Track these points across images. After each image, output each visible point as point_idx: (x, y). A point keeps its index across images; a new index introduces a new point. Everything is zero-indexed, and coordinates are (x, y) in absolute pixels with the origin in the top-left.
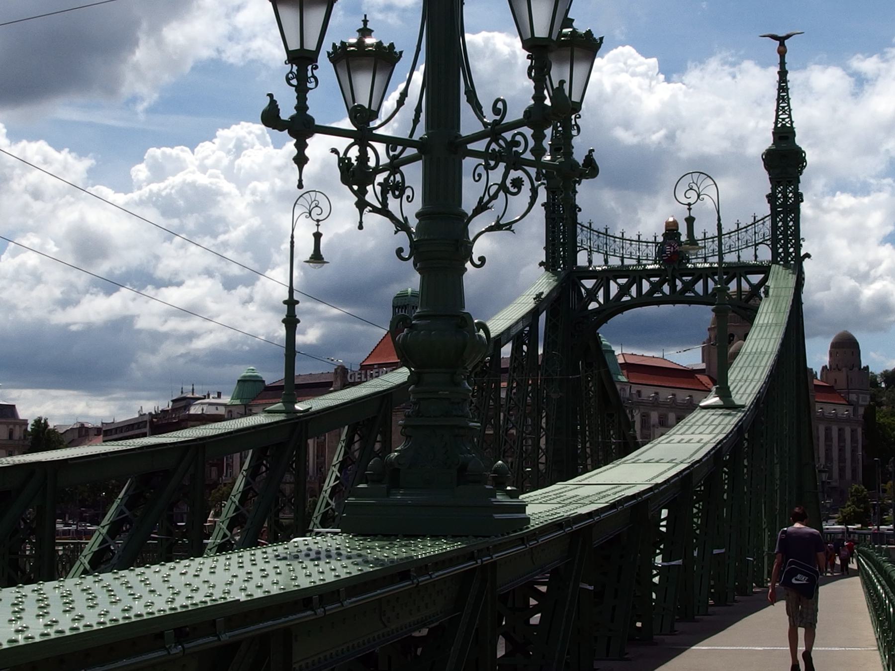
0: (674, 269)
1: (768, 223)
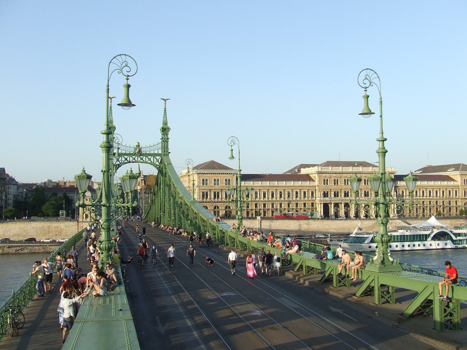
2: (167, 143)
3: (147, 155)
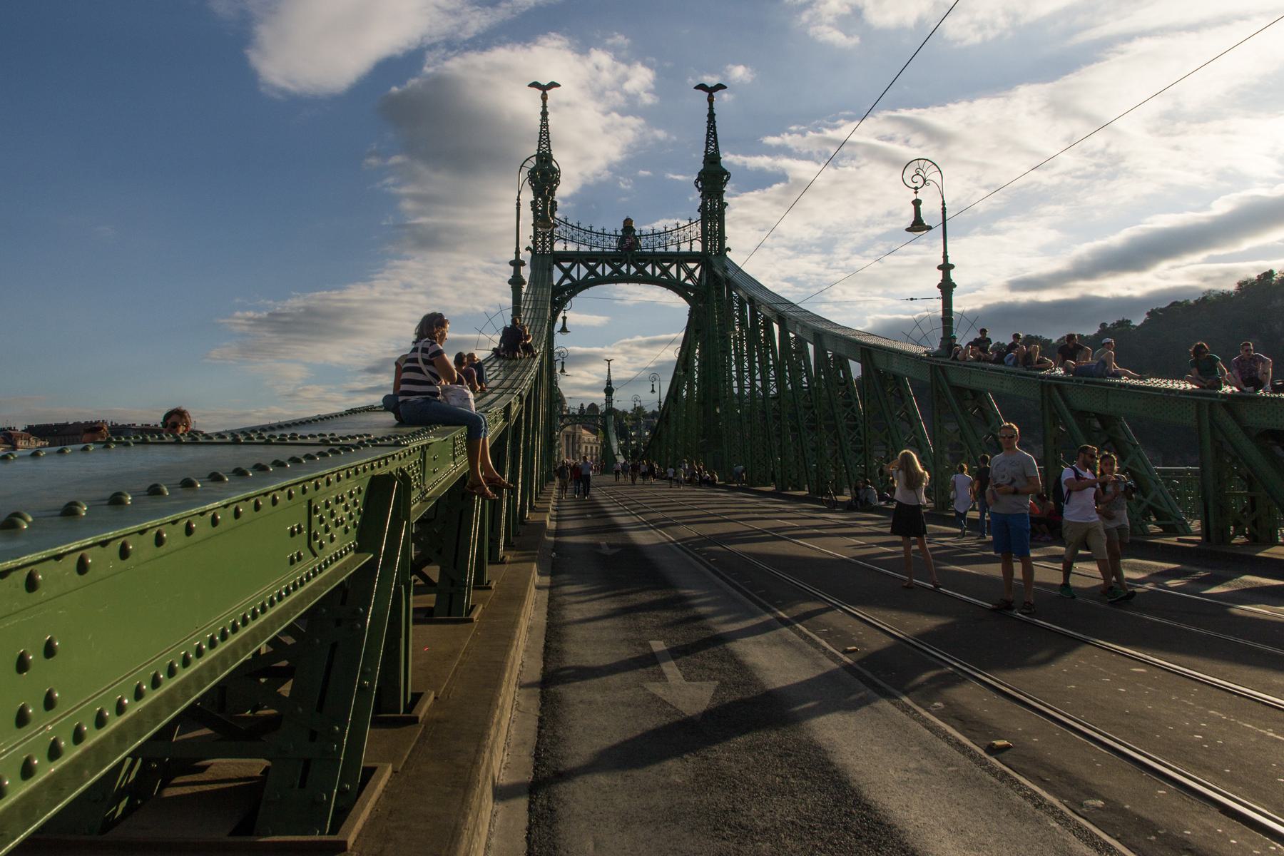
0: (633, 255)
1: (700, 225)
3: (657, 259)
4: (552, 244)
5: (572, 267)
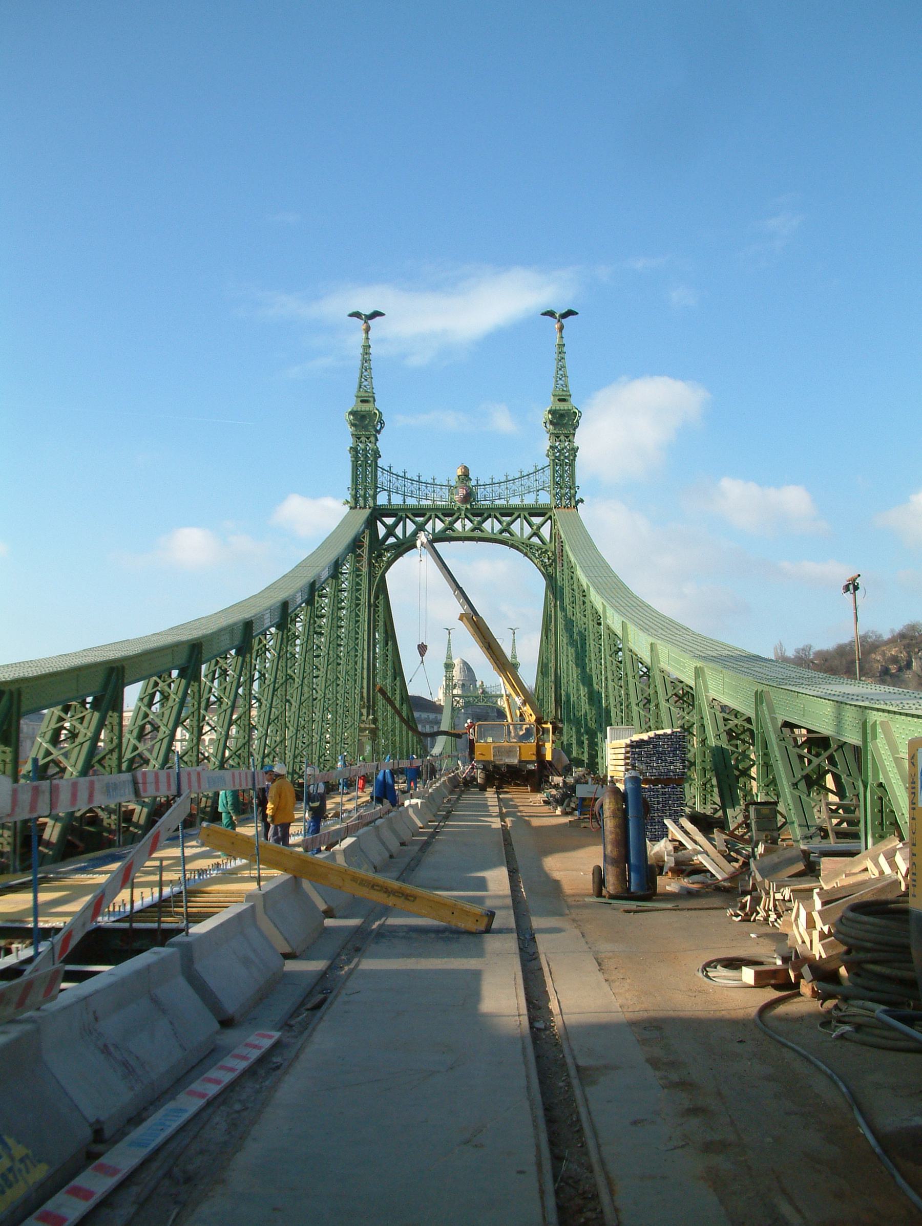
0: (467, 509)
1: (548, 472)
2: (572, 465)
4: (374, 498)
5: (396, 525)
